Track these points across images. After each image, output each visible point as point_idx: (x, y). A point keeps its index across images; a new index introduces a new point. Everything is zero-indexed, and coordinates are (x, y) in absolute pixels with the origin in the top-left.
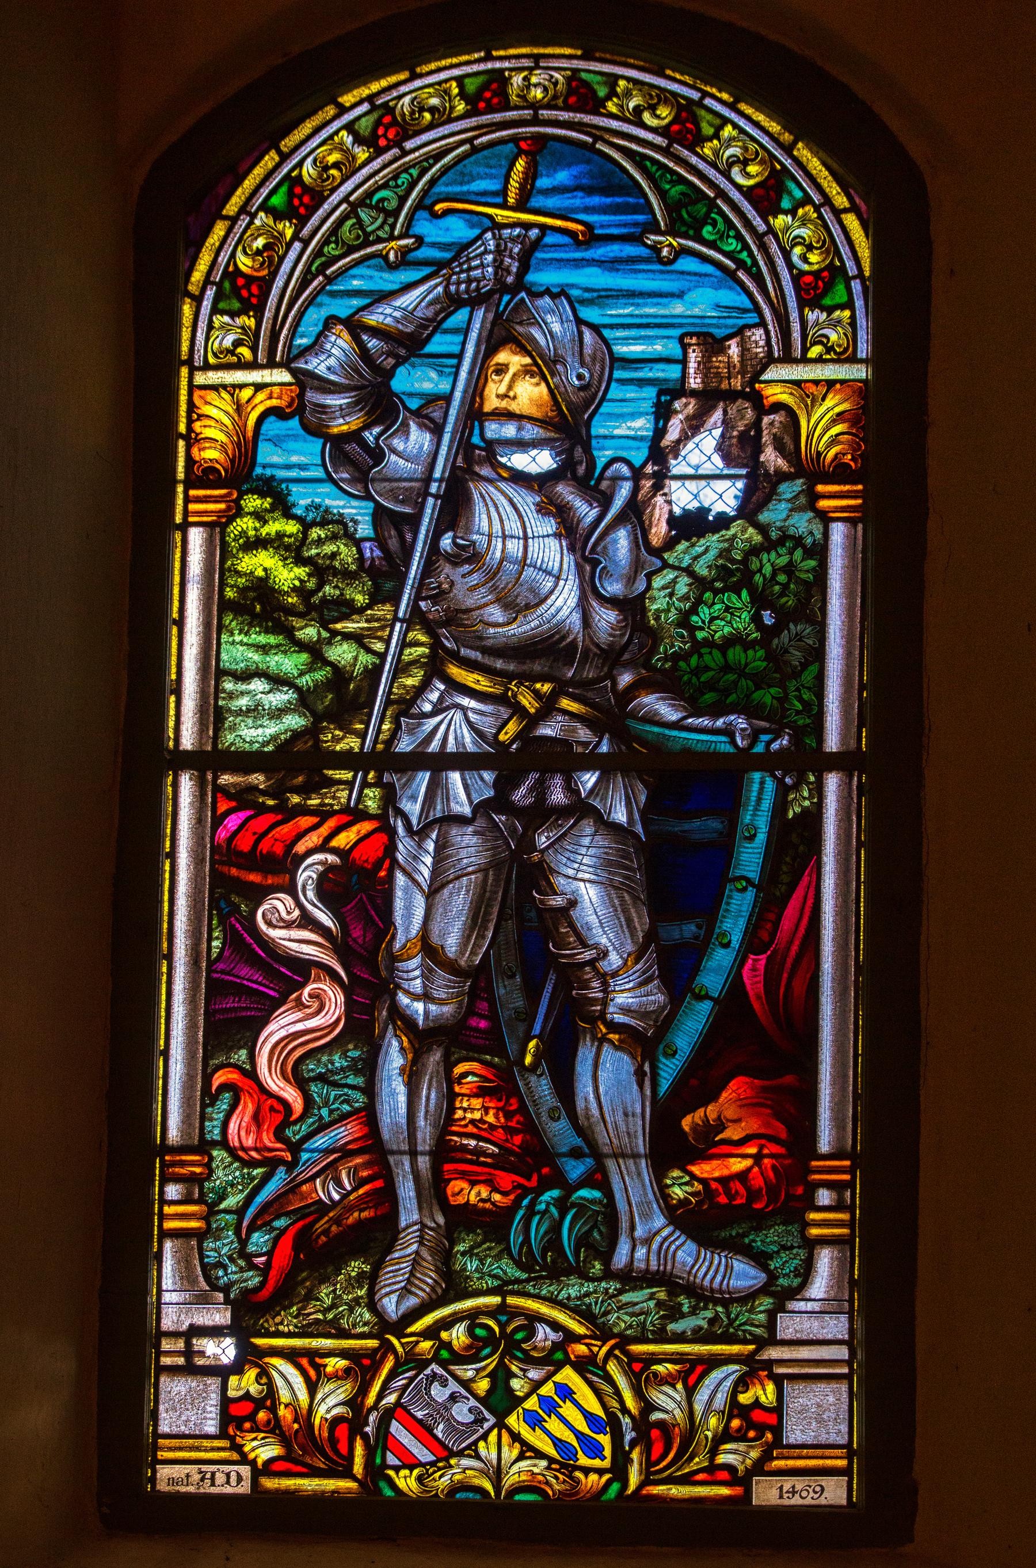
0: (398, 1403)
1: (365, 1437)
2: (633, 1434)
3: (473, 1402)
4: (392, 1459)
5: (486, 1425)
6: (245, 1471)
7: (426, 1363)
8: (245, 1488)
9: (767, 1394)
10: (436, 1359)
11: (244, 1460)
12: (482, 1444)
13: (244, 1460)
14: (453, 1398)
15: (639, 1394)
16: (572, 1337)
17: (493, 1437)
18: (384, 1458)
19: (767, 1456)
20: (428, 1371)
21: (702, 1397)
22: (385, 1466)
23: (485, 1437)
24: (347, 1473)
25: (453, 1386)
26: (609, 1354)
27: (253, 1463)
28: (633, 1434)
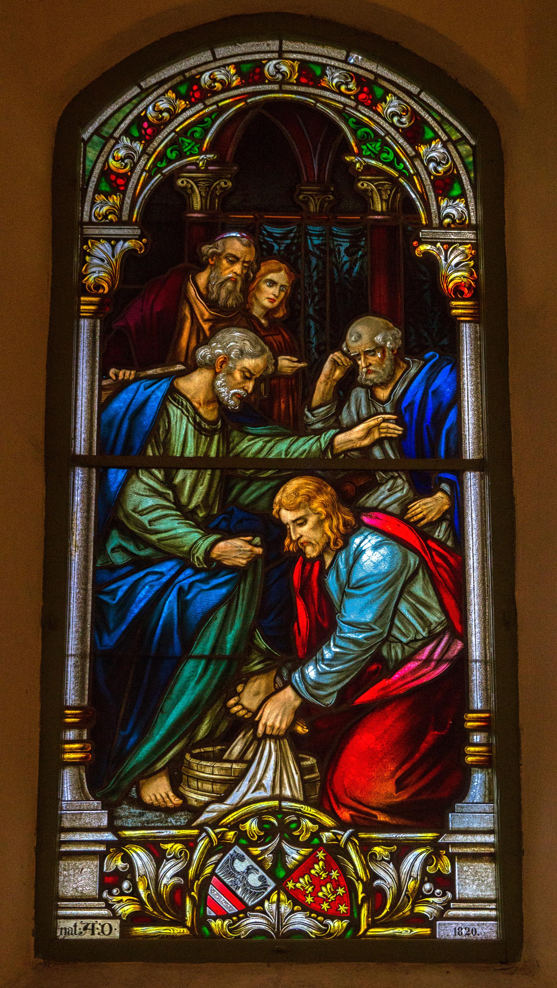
0: (213, 873)
1: (192, 898)
2: (363, 895)
3: (261, 873)
4: (210, 912)
5: (269, 889)
6: (116, 924)
7: (231, 846)
8: (116, 934)
9: (445, 866)
10: (237, 843)
11: (115, 916)
12: (266, 904)
13: (115, 916)
14: (249, 870)
15: (366, 867)
16: (324, 828)
17: (274, 897)
18: (205, 910)
19: (447, 907)
20: (231, 852)
21: (405, 867)
22: (206, 917)
23: (268, 898)
24: (181, 923)
25: (248, 862)
26: (349, 839)
27: (119, 917)
28: (363, 895)
